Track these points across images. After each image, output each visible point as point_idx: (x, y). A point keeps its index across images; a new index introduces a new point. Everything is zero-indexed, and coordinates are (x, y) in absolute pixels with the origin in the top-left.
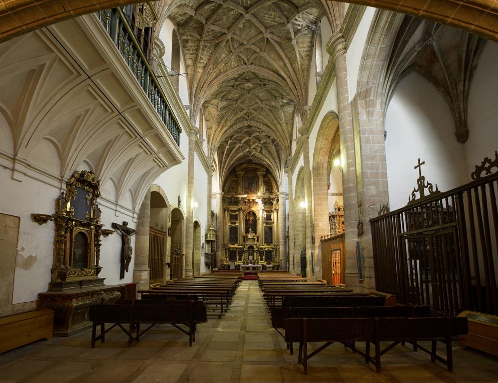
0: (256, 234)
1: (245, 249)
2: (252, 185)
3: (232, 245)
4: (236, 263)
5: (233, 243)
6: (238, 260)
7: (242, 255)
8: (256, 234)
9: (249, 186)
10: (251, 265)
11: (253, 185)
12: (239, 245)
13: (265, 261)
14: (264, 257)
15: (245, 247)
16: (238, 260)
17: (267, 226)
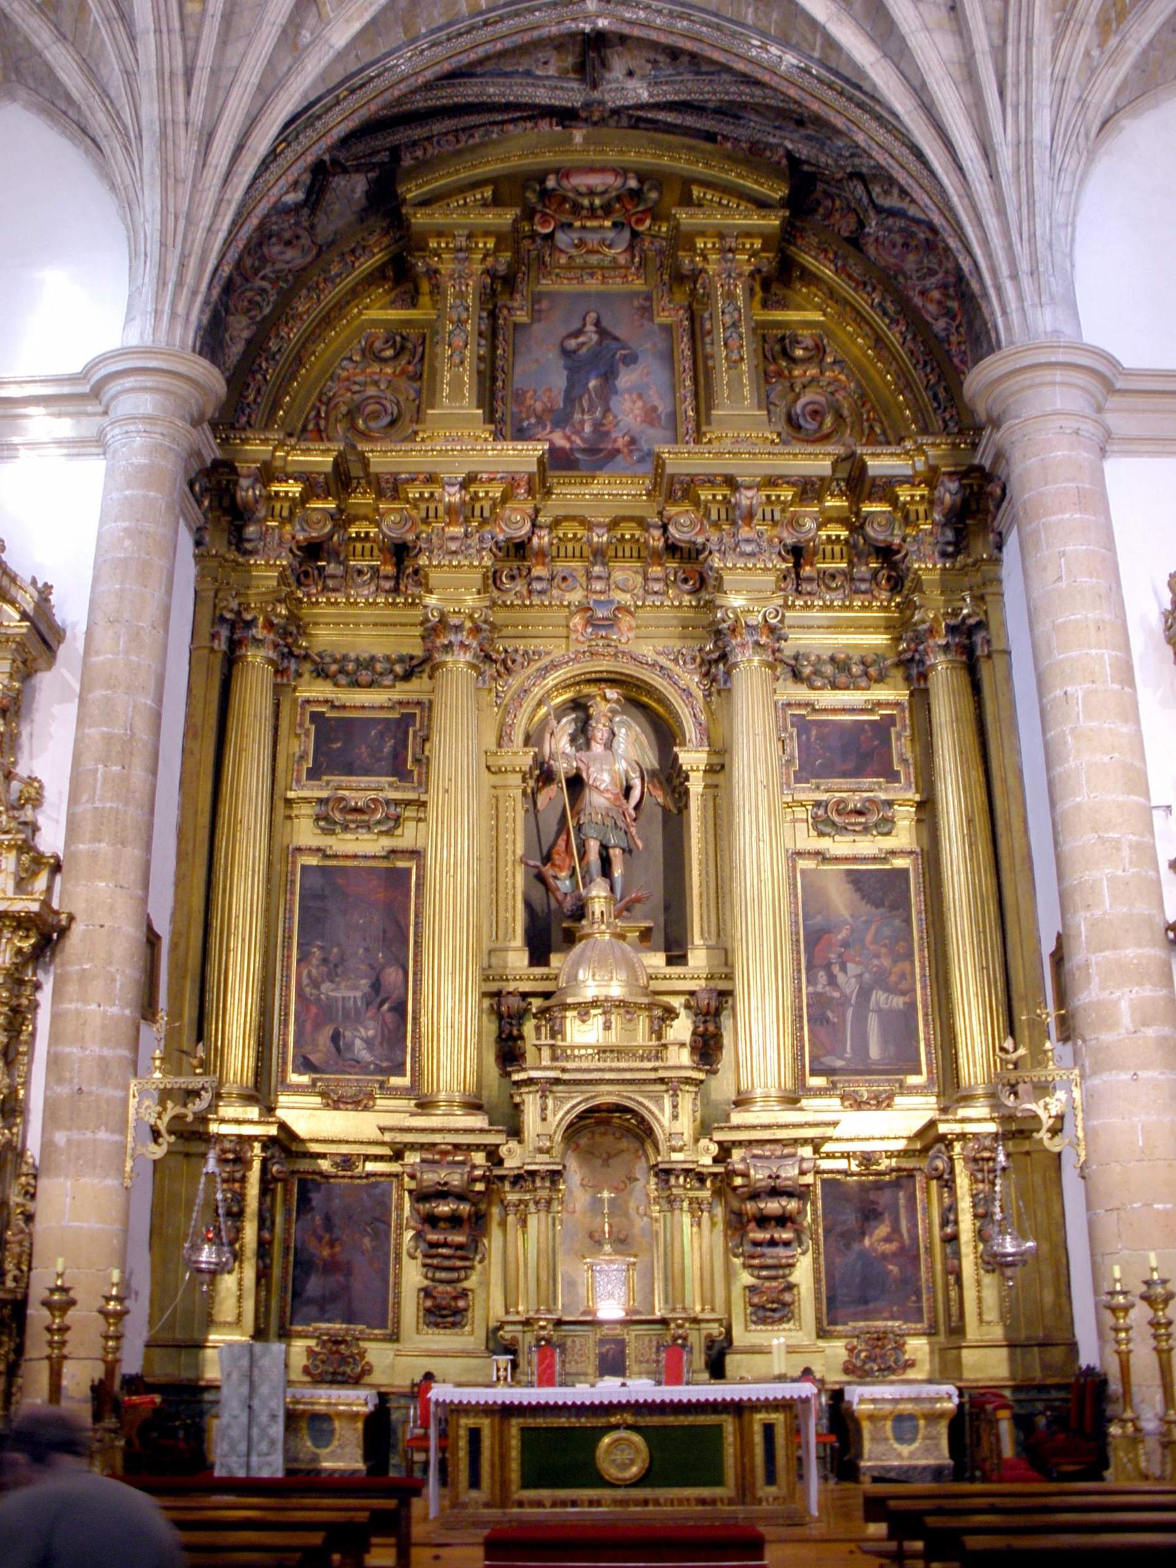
0: (676, 957)
1: (514, 1157)
2: (609, 376)
3: (335, 1102)
4: (377, 1354)
5: (350, 1082)
6: (410, 1308)
7: (469, 1252)
8: (676, 957)
9: (571, 398)
10: (609, 1389)
11: (626, 379)
12: (425, 1105)
13: (822, 1334)
14: (803, 1272)
15: (515, 1132)
16: (410, 1308)
17: (839, 846)
